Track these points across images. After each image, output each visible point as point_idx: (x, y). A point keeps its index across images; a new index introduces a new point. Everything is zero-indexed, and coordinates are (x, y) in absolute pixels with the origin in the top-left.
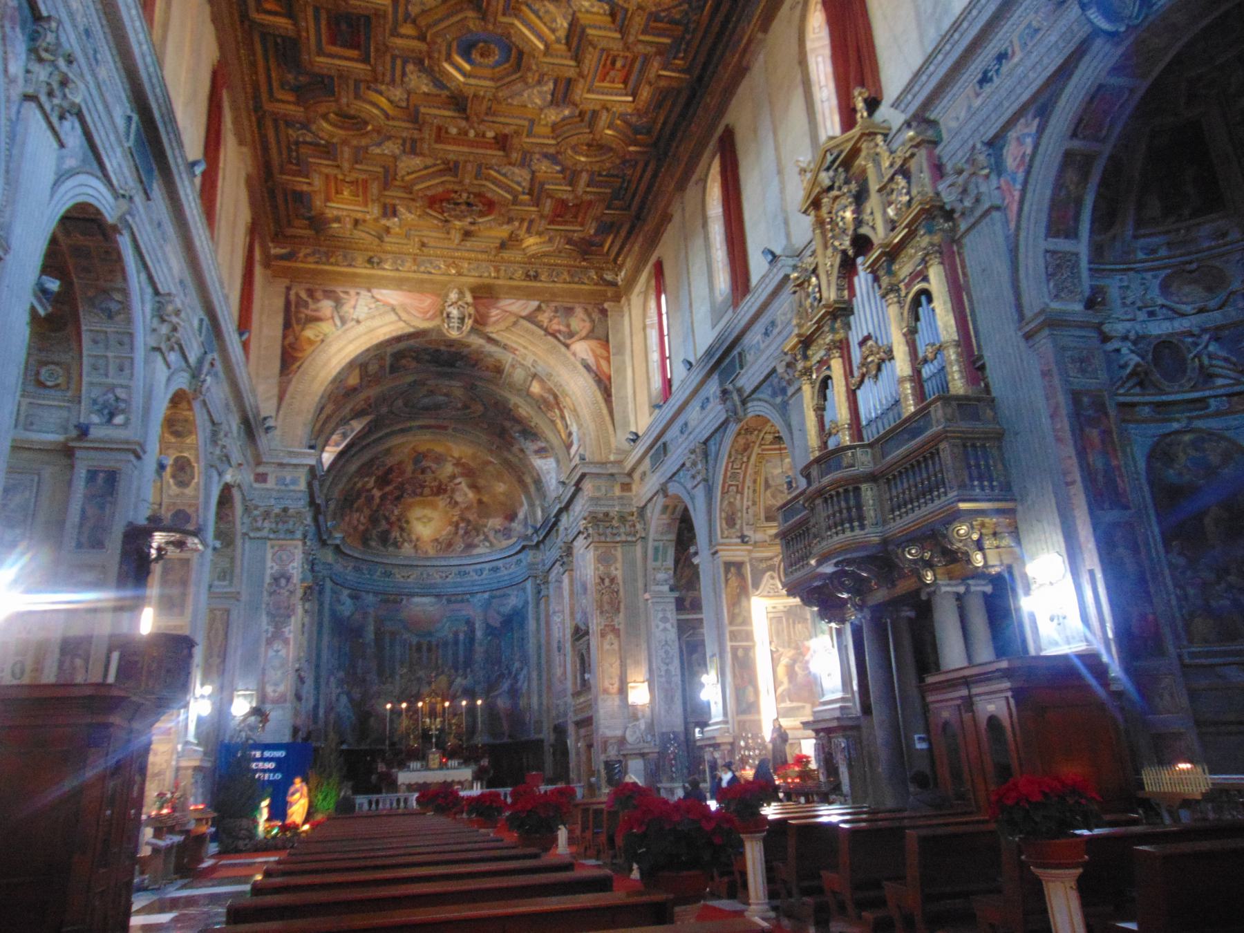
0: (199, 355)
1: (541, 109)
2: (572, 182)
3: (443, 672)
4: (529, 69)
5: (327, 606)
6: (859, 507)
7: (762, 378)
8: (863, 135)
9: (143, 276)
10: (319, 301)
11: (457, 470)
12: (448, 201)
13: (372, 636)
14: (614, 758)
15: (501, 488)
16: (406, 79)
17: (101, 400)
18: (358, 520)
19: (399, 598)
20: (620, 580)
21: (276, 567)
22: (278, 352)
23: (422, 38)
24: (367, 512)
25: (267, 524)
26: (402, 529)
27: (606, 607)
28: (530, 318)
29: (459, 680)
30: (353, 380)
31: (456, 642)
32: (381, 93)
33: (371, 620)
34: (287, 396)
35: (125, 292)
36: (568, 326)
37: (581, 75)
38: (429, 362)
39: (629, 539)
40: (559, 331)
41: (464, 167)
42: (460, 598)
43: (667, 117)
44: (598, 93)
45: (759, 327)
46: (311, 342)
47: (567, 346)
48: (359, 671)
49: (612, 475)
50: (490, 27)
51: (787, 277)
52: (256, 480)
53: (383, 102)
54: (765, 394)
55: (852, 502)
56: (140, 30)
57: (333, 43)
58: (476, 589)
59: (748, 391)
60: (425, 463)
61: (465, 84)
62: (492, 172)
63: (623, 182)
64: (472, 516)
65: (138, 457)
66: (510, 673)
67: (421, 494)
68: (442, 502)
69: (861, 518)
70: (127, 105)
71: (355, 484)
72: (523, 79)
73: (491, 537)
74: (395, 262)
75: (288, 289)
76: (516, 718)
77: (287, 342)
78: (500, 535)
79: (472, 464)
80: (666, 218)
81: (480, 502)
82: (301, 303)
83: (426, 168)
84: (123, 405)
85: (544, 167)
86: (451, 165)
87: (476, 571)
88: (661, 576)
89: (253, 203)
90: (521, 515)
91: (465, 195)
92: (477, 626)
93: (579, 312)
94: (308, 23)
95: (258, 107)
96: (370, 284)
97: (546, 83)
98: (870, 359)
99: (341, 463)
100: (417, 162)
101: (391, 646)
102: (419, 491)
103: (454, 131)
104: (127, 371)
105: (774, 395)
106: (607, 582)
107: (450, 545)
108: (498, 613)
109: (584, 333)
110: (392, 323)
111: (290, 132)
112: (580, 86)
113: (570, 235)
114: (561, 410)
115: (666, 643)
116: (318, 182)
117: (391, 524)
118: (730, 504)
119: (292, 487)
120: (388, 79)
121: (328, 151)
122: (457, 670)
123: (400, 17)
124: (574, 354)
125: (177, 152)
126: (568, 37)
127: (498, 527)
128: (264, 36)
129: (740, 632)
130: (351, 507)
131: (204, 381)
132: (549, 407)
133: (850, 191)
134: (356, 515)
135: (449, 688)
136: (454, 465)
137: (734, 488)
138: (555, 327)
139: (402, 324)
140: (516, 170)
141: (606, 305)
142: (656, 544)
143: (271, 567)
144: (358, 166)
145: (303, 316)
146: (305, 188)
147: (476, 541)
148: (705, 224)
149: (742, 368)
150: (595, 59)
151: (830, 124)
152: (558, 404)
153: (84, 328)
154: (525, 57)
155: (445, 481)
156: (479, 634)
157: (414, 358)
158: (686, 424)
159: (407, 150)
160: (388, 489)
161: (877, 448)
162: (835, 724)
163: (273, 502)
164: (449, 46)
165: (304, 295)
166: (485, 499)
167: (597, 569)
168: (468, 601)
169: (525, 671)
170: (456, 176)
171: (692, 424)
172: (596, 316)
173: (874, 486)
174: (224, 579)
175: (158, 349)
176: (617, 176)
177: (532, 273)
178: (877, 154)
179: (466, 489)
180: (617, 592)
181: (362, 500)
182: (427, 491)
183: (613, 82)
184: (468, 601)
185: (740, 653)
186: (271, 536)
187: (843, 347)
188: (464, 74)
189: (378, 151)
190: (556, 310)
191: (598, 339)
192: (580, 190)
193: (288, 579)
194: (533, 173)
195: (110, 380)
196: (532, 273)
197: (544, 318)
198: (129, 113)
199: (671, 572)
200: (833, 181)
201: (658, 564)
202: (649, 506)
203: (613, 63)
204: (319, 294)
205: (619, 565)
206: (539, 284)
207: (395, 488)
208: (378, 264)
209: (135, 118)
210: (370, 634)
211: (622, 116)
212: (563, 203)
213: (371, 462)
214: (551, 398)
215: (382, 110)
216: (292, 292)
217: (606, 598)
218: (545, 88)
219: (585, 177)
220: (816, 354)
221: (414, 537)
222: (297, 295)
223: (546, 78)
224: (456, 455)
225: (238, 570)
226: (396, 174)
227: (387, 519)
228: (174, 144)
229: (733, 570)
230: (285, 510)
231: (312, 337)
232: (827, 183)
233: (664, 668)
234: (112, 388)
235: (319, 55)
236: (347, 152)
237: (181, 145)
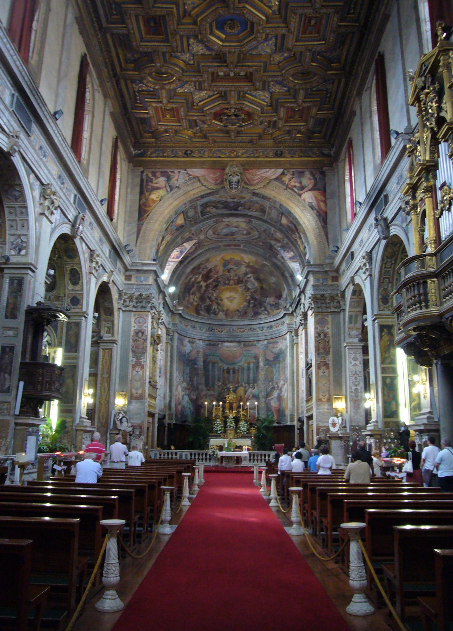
0: (75, 214)
1: (270, 55)
2: (295, 96)
3: (241, 385)
4: (258, 32)
5: (175, 348)
6: (426, 294)
7: (396, 211)
8: (439, 52)
9: (32, 176)
10: (158, 178)
11: (248, 270)
12: (224, 114)
13: (202, 364)
14: (323, 438)
15: (273, 280)
16: (190, 48)
17: (15, 243)
18: (194, 299)
19: (217, 343)
20: (330, 334)
21: (137, 327)
22: (137, 208)
23: (195, 23)
24: (198, 295)
25: (132, 304)
26: (218, 304)
27: (321, 351)
28: (277, 179)
29: (250, 389)
30: (180, 221)
31: (249, 369)
32: (178, 58)
33: (201, 355)
34: (142, 232)
35: (21, 185)
36: (301, 183)
37: (289, 31)
38: (222, 208)
39: (336, 310)
40: (295, 186)
41: (230, 94)
42: (250, 343)
43: (348, 51)
44: (302, 41)
45: (394, 179)
46: (154, 201)
47: (300, 195)
48: (195, 383)
49: (326, 272)
50: (232, 11)
51: (405, 147)
52: (126, 279)
53: (181, 63)
54: (398, 221)
55: (421, 291)
56: (10, 49)
57: (148, 33)
58: (260, 338)
59: (390, 219)
60: (229, 267)
61: (222, 46)
62: (247, 95)
63: (327, 94)
64: (257, 297)
65: (33, 272)
66: (278, 387)
67: (228, 284)
68: (240, 288)
69: (426, 301)
70: (11, 88)
71: (191, 279)
72: (255, 39)
74: (200, 152)
75: (142, 172)
76: (281, 412)
77: (142, 202)
78: (273, 307)
79: (257, 266)
80: (353, 114)
81: (262, 288)
82: (150, 180)
83: (209, 97)
84: (25, 245)
85: (276, 89)
86: (223, 94)
87: (259, 328)
88: (354, 333)
89: (117, 127)
90: (284, 296)
91: (233, 110)
92: (260, 360)
93: (307, 174)
94: (133, 24)
95: (115, 75)
96: (186, 166)
97: (271, 39)
98: (445, 198)
99: (180, 268)
100: (203, 94)
101: (213, 370)
102: (227, 282)
103: (221, 74)
104: (26, 227)
105: (402, 222)
106: (322, 335)
107: (245, 313)
108: (272, 352)
109: (310, 187)
110: (198, 187)
111: (134, 85)
112: (291, 38)
113: (299, 128)
114: (299, 233)
115: (356, 372)
116: (151, 112)
117: (212, 301)
118: (385, 289)
119: (144, 283)
120: (180, 48)
121: (153, 94)
122: (249, 384)
123: (181, 13)
124: (304, 200)
125: (43, 109)
126: (279, 10)
127: (272, 303)
128: (112, 35)
129: (388, 368)
130: (189, 292)
131: (78, 228)
132: (293, 232)
133: (434, 89)
134: (192, 297)
135: (245, 394)
136: (246, 267)
137: (387, 280)
138: (293, 184)
139: (204, 188)
140: (261, 93)
141: (324, 169)
142: (351, 313)
143: (134, 327)
144: (172, 101)
145: (150, 187)
146: (146, 116)
148: (371, 117)
149: (386, 204)
150: (297, 20)
151: (428, 48)
152: (297, 229)
153: (5, 206)
154: (255, 25)
155: (241, 276)
156: (261, 364)
157: (214, 207)
158: (362, 241)
159: (197, 88)
160: (209, 282)
161: (439, 255)
162: (422, 428)
163: (134, 291)
164: (211, 26)
165: (150, 175)
166: (264, 286)
167: (316, 328)
168: (255, 345)
169: (285, 386)
170: (226, 100)
171: (365, 240)
172: (317, 176)
173: (436, 280)
174: (110, 333)
175: (42, 214)
176: (322, 90)
177: (279, 153)
178: (450, 63)
179: (253, 281)
180: (328, 342)
181: (194, 289)
182: (232, 282)
183: (311, 33)
184: (255, 345)
185: (388, 381)
186: (134, 309)
187: (431, 190)
188: (222, 41)
189: (180, 90)
190: (293, 174)
191: (319, 190)
192: (300, 101)
193: (143, 333)
194: (271, 93)
195: (18, 232)
196: (279, 153)
197: (286, 179)
198: (13, 92)
199: (360, 331)
200: (424, 82)
201: (352, 326)
202: (347, 290)
203: (309, 22)
204: (158, 174)
205: (329, 326)
206: (283, 159)
207: (214, 281)
208: (190, 154)
209: (16, 94)
210: (200, 363)
211: (320, 53)
212: (292, 109)
213: (198, 267)
214: (293, 227)
215: (180, 67)
216: (144, 174)
217: (321, 345)
218: (271, 42)
219: (302, 93)
220: (420, 194)
221: (225, 309)
222: (147, 175)
223: (270, 36)
224: (247, 261)
225: (116, 328)
226: (194, 103)
227: (210, 298)
228: (41, 105)
229: (385, 330)
230: (141, 295)
231: (155, 198)
232: (421, 84)
233: (354, 388)
234: (19, 236)
235: (141, 42)
236: (164, 93)
237: (45, 105)
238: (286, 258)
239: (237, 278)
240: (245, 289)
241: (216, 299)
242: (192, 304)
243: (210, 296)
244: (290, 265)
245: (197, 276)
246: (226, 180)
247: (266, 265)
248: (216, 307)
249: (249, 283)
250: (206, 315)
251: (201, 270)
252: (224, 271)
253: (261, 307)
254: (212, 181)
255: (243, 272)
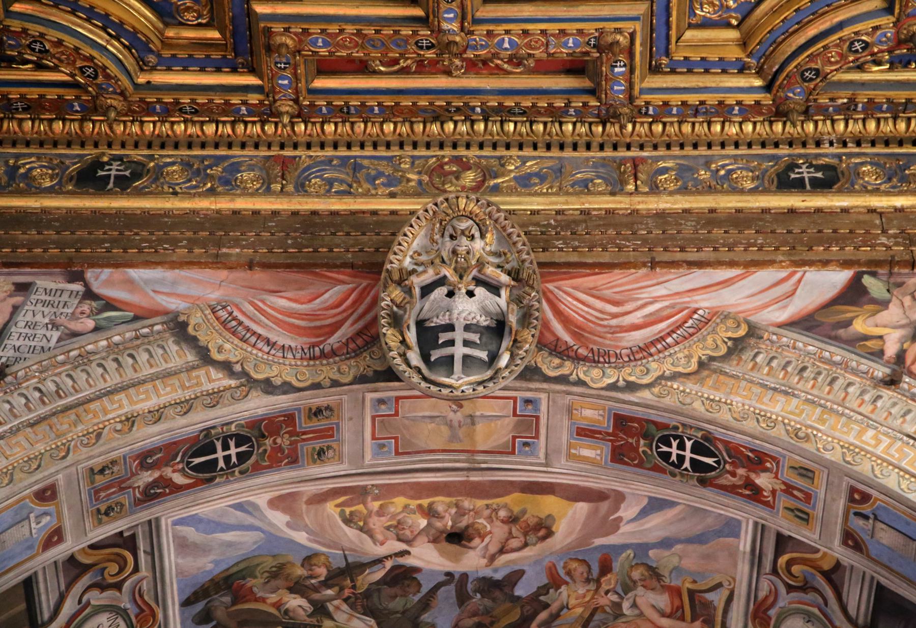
139: (218, 380)
246: (397, 322)
254: (284, 339)
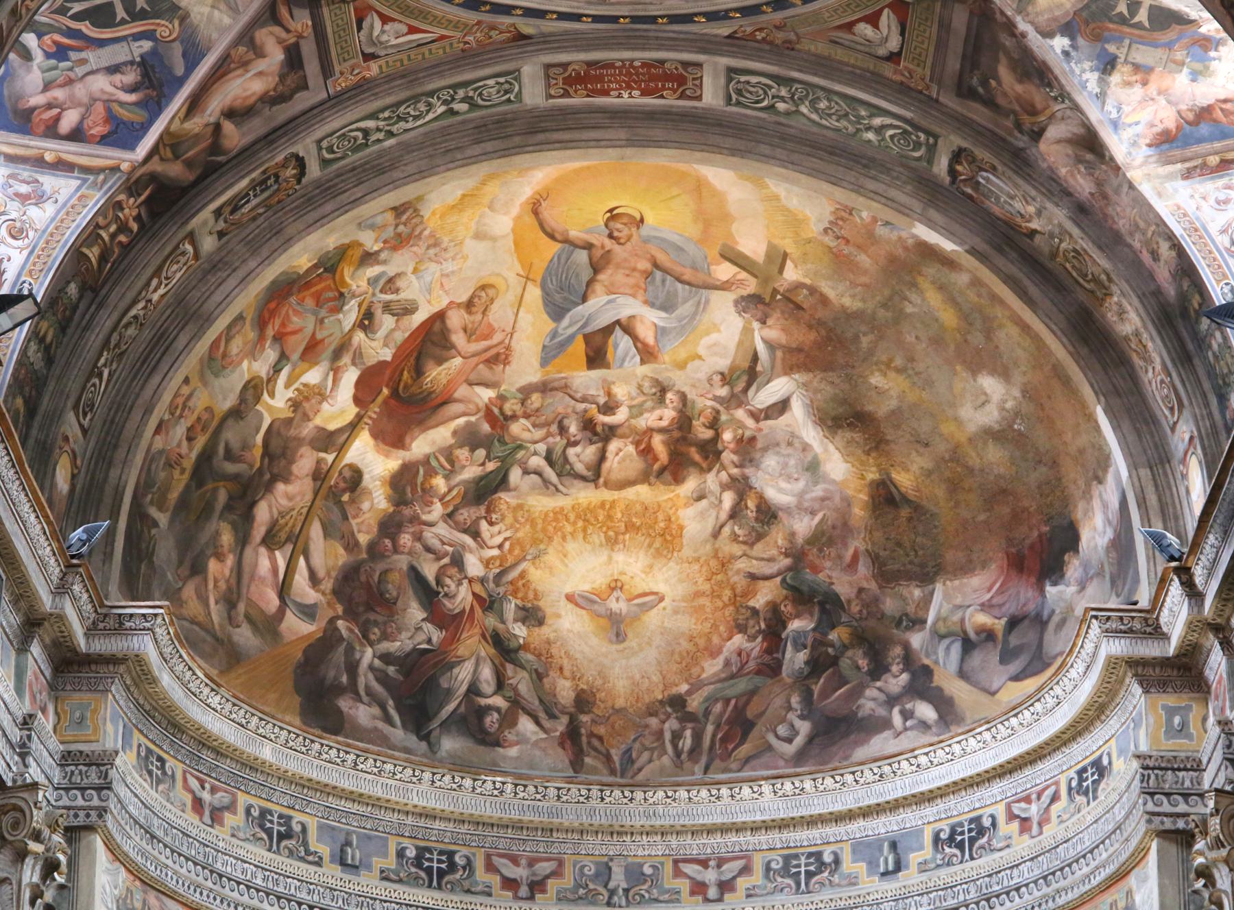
18: (283, 590)
26: (504, 649)
67: (595, 474)
71: (254, 390)
73: (947, 680)
78: (986, 660)
79: (840, 295)
87: (865, 849)
117: (450, 622)
134: (265, 563)
147: (869, 703)
155: (703, 403)
160: (423, 444)
166: (904, 480)
179: (811, 435)
182: (622, 455)
207: (470, 439)
221: (565, 691)
227: (429, 595)
238: (1118, 145)
239: (668, 414)
240: (735, 514)
241: (489, 604)
242: (268, 626)
243: (429, 571)
244: (1163, 208)
245: (313, 376)
247: (928, 252)
248: (487, 673)
249: (771, 462)
250: (398, 734)
251: (350, 314)
252: (552, 352)
253: (878, 669)
255: (724, 364)
